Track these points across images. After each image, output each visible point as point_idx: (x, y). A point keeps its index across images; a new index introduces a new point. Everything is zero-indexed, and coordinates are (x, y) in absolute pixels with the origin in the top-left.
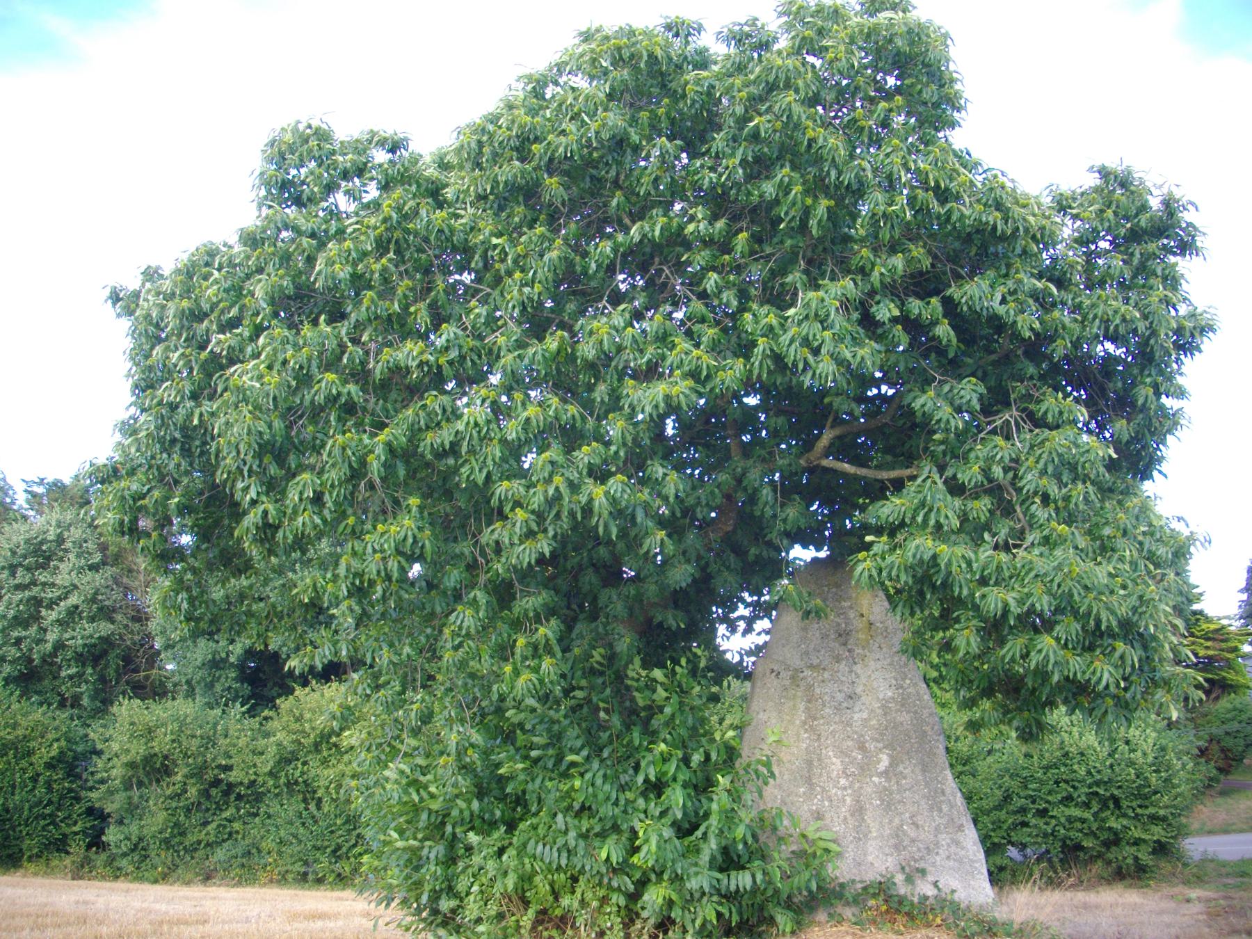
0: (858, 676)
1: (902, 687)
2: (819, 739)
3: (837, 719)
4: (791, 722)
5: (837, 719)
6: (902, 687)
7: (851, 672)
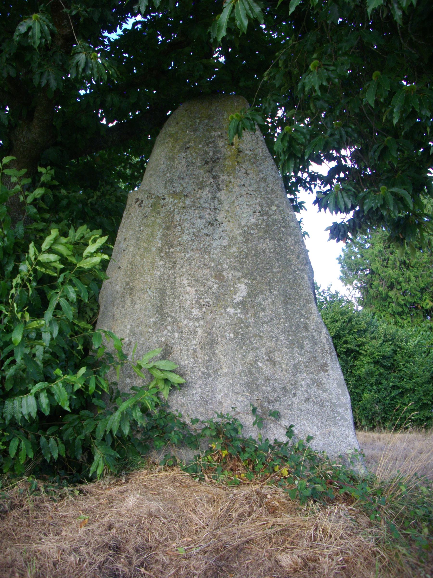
0: (221, 202)
1: (267, 213)
2: (173, 267)
3: (195, 246)
4: (148, 250)
5: (195, 246)
6: (267, 213)
7: (214, 198)
